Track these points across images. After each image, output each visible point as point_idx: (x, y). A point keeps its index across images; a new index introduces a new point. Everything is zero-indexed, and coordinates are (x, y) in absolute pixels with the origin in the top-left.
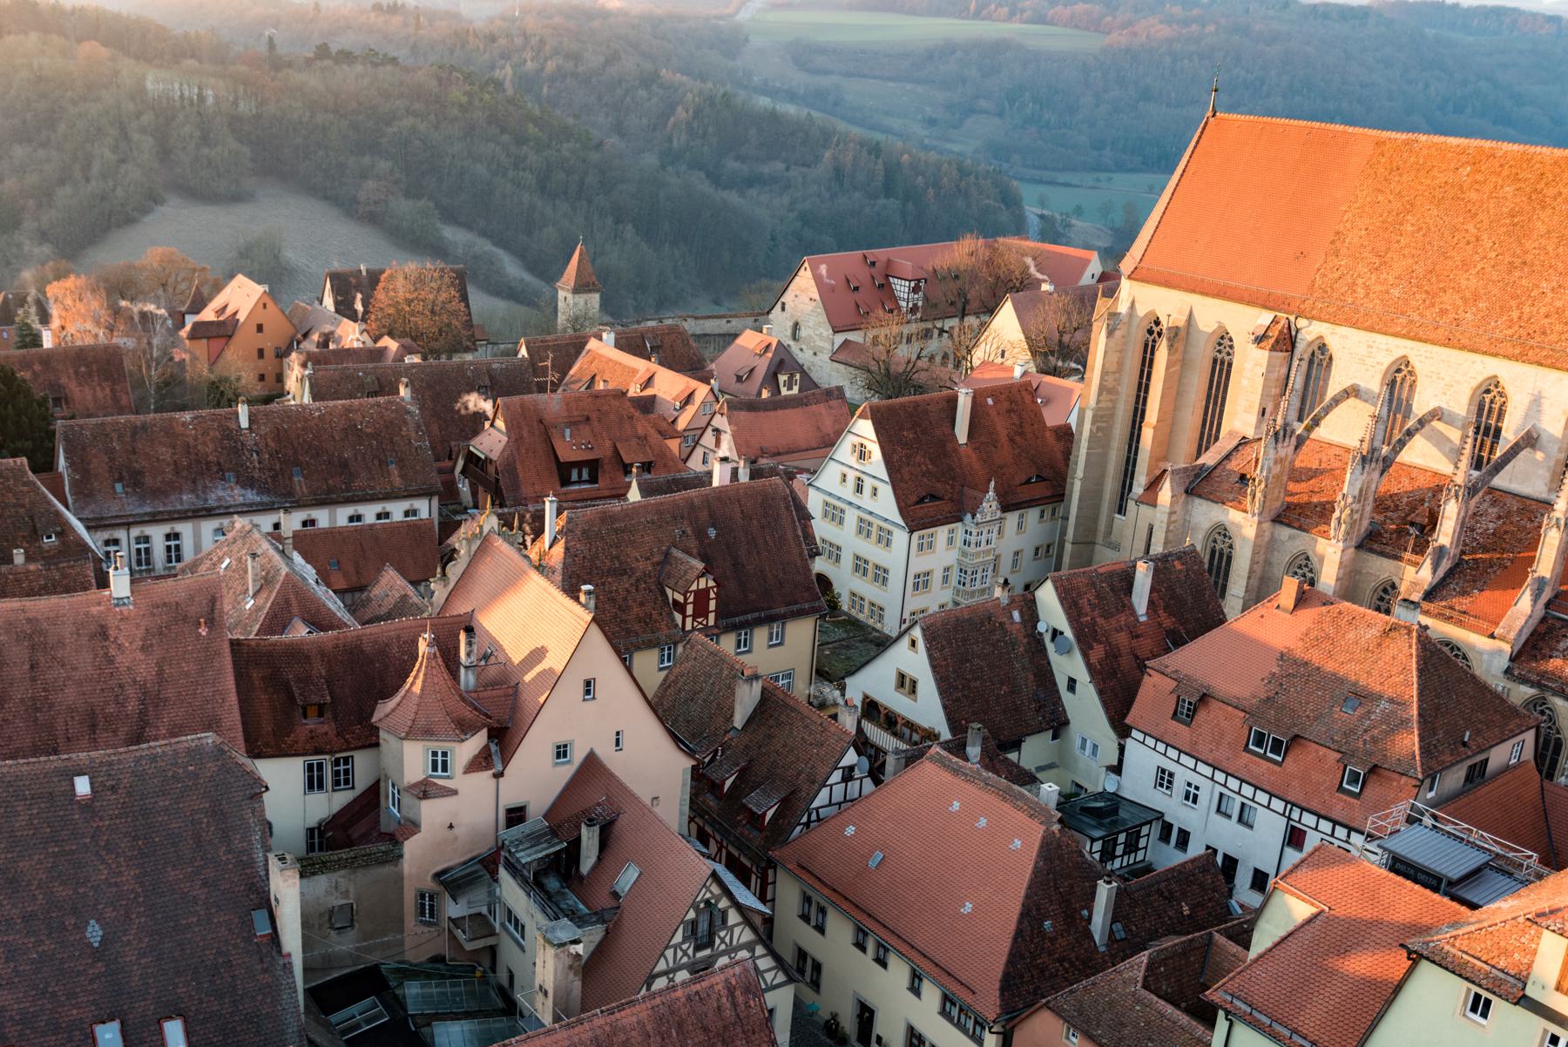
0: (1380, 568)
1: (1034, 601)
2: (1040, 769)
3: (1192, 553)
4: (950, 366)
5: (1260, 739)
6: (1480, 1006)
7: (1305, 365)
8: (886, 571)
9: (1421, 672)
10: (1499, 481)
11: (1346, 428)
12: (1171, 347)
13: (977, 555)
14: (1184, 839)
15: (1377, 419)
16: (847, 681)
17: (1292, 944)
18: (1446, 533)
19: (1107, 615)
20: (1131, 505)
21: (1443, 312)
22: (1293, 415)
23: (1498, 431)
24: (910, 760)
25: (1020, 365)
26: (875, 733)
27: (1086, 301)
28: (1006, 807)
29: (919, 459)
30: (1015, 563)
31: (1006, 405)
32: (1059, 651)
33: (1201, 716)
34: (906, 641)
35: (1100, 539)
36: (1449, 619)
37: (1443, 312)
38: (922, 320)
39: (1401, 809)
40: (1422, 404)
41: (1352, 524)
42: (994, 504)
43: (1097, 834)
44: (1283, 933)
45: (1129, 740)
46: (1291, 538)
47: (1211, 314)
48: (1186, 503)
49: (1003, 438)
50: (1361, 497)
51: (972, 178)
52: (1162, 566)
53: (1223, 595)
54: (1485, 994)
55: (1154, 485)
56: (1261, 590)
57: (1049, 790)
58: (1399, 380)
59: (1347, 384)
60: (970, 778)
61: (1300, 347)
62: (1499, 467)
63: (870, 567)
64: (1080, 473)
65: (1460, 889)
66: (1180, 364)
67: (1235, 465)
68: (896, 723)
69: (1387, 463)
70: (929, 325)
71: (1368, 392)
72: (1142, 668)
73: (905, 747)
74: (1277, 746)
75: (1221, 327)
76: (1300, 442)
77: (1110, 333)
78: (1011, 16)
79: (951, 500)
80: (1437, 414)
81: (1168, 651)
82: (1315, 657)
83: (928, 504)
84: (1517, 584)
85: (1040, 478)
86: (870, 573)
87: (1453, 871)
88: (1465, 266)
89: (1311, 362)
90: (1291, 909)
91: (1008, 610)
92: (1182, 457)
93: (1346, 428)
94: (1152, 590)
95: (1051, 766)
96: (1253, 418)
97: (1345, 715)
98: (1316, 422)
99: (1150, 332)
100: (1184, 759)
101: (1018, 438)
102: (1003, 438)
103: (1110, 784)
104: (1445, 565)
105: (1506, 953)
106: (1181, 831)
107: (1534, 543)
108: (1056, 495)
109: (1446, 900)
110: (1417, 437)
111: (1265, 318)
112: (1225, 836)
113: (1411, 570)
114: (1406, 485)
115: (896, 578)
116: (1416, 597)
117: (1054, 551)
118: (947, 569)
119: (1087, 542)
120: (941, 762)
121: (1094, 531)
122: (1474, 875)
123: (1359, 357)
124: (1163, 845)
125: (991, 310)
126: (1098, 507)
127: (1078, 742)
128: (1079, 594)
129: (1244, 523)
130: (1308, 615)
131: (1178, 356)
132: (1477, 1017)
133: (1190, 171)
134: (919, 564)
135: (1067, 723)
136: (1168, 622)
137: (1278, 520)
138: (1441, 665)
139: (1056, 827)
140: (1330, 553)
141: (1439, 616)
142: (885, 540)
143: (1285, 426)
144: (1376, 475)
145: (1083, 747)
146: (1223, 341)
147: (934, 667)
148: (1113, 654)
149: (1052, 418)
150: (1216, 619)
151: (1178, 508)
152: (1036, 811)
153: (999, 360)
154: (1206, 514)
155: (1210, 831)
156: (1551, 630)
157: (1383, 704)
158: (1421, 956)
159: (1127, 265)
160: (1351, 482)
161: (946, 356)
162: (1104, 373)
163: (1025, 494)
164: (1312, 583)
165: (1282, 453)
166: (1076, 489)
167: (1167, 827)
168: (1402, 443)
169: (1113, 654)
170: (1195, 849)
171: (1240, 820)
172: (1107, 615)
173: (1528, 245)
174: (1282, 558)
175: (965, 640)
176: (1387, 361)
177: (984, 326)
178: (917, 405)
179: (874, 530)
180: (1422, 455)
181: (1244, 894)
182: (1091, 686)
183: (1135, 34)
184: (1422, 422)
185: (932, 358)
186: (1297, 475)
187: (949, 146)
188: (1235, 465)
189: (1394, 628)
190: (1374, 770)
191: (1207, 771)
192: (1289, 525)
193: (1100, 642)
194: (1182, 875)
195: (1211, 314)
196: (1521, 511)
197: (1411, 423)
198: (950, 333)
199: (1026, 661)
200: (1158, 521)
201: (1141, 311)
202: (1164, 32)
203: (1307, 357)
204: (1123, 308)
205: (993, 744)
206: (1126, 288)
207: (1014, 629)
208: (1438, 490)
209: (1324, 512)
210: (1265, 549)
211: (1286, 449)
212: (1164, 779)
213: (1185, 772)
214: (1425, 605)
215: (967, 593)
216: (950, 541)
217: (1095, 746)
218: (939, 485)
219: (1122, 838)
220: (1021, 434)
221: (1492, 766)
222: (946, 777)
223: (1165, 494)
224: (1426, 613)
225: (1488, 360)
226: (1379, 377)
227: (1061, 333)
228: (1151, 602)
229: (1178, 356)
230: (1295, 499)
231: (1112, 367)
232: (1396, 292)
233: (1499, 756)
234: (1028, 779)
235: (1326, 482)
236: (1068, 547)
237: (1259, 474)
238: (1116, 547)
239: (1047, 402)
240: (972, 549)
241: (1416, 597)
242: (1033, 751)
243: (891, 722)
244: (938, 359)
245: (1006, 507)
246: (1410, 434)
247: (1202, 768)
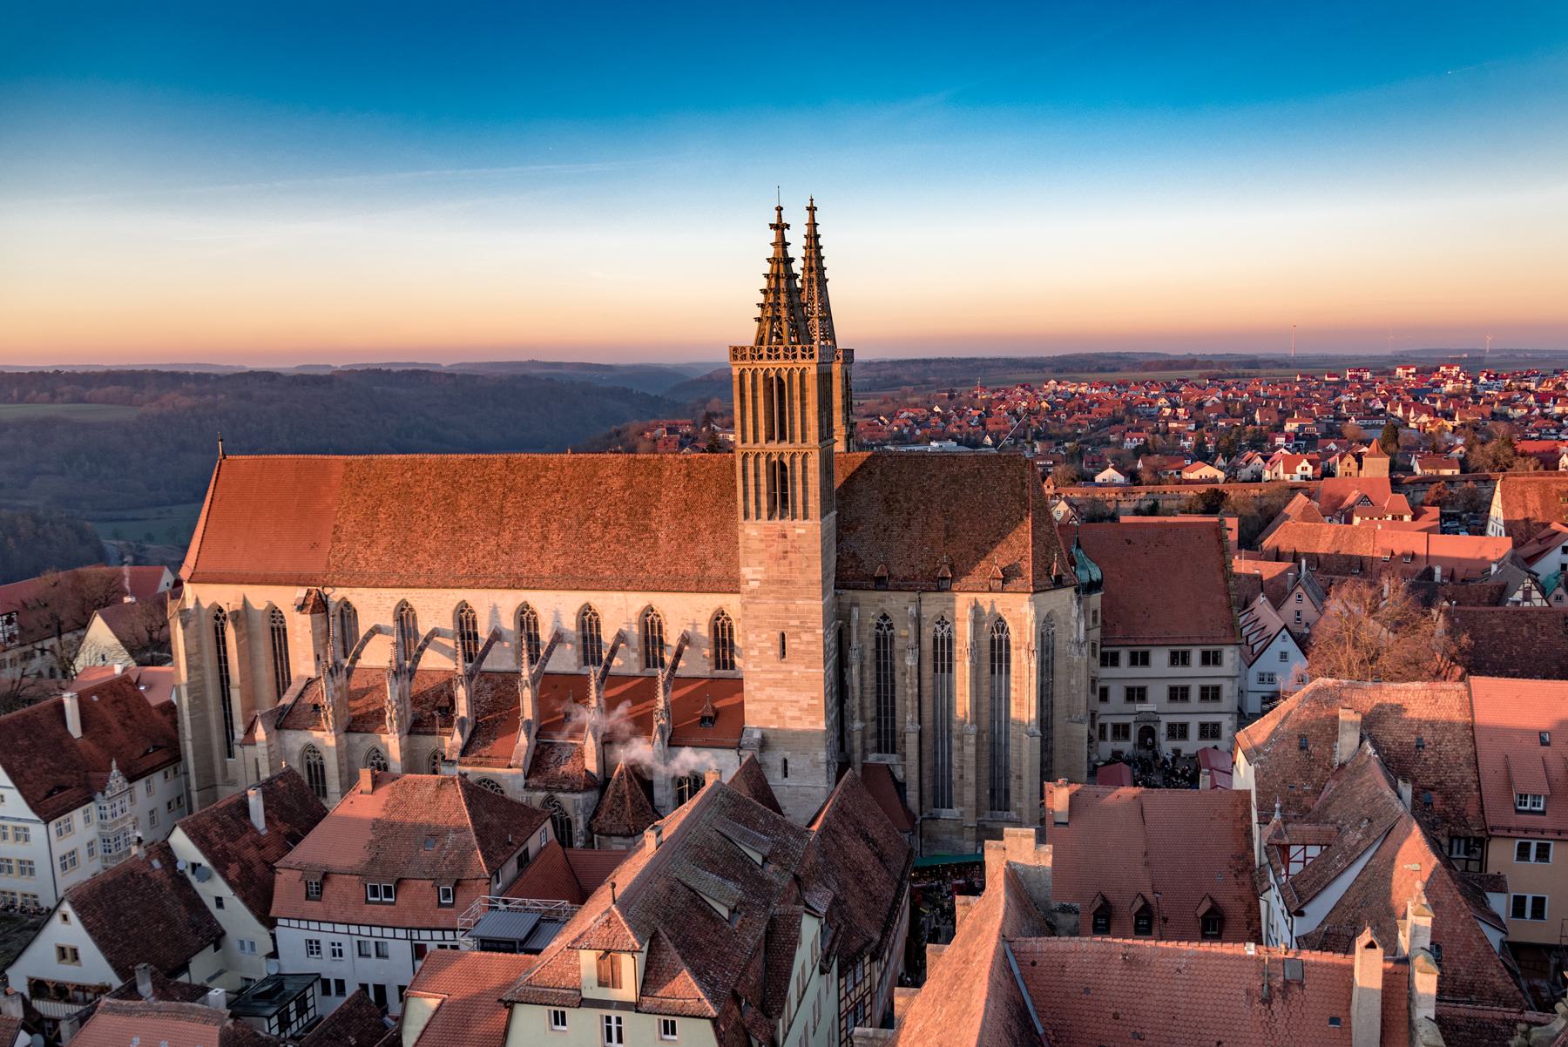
0: (427, 743)
1: (169, 847)
2: (210, 979)
3: (289, 774)
4: (59, 677)
5: (375, 893)
6: (559, 1019)
7: (338, 619)
8: (30, 863)
9: (469, 806)
10: (486, 666)
11: (378, 655)
12: (235, 626)
13: (116, 823)
14: (341, 985)
15: (396, 644)
16: (8, 972)
17: (431, 1033)
18: (462, 709)
19: (234, 839)
20: (237, 749)
21: (420, 566)
22: (340, 655)
23: (476, 635)
24: (83, 1019)
25: (120, 664)
26: (44, 1007)
27: (162, 606)
28: (182, 1024)
29: (38, 760)
30: (152, 820)
31: (111, 698)
32: (202, 879)
33: (328, 889)
34: (57, 918)
35: (219, 781)
36: (480, 764)
37: (420, 566)
38: (22, 645)
39: (478, 904)
40: (424, 628)
41: (400, 719)
42: (121, 779)
43: (270, 1011)
44: (421, 1028)
45: (278, 929)
46: (362, 740)
47: (259, 597)
48: (278, 737)
49: (115, 724)
50: (401, 700)
51: (48, 525)
52: (268, 789)
53: (325, 795)
54: (560, 1009)
55: (250, 729)
56: (350, 781)
57: (217, 994)
58: (404, 616)
59: (371, 626)
60: (143, 1014)
61: (332, 607)
62: (482, 658)
63: (14, 864)
64: (188, 735)
65: (527, 945)
66: (246, 638)
67: (308, 699)
68: (67, 991)
69: (412, 672)
70: (28, 648)
71: (387, 628)
72: (272, 869)
73: (77, 1008)
74: (388, 893)
75: (271, 604)
76: (349, 672)
77: (184, 626)
78: (53, 398)
79: (79, 786)
80: (435, 633)
81: (290, 849)
82: (396, 817)
83: (57, 795)
84: (515, 729)
85: (156, 748)
86: (15, 870)
87: (521, 934)
88: (425, 534)
89: (342, 616)
90: (423, 1007)
91: (148, 861)
92: (267, 703)
93: (378, 655)
94: (266, 808)
95: (220, 973)
96: (312, 664)
97: (428, 853)
98: (357, 656)
99: (217, 618)
100: (324, 926)
101: (128, 722)
102: (115, 724)
103: (271, 968)
104: (468, 729)
105: (563, 975)
106: (337, 981)
107: (517, 701)
108: (176, 757)
109: (521, 955)
110: (427, 650)
111: (301, 592)
112: (371, 971)
113: (447, 739)
114: (428, 684)
115: (42, 867)
116: (455, 756)
117: (184, 800)
118: (90, 844)
119: (209, 786)
120: (113, 1010)
121: (213, 776)
122: (535, 930)
123: (374, 607)
124: (326, 998)
125: (84, 625)
126: (211, 758)
127: (237, 945)
128: (207, 830)
129: (326, 738)
130: (384, 792)
131: (244, 631)
132: (560, 1027)
133: (218, 495)
134: (61, 847)
135: (223, 933)
136: (285, 828)
137: (349, 730)
138: (481, 795)
139: (229, 1023)
140: (392, 742)
141: (474, 764)
142: (22, 835)
143: (335, 663)
144: (407, 682)
145: (242, 948)
146: (274, 613)
147: (90, 931)
148: (247, 867)
149: (155, 699)
150: (322, 813)
151: (273, 741)
152: (207, 1018)
153: (101, 663)
154: (296, 740)
155: (357, 972)
156: (543, 752)
157: (452, 836)
158: (513, 1002)
159: (185, 573)
160: (391, 692)
161: (52, 670)
162: (188, 656)
163: (146, 764)
164: (386, 768)
165: (339, 683)
166: (189, 748)
167: (326, 983)
168: (418, 657)
169: (247, 867)
170: (351, 989)
171: (378, 955)
172: (234, 839)
173: (460, 515)
174: (360, 756)
175: (113, 899)
176: (393, 605)
177: (81, 639)
178: (25, 716)
179: (10, 831)
180: (434, 661)
181: (394, 1007)
182: (236, 899)
183: (162, 405)
184: (427, 640)
185: (40, 674)
186: (355, 695)
187: (20, 503)
188: (308, 699)
189: (444, 782)
190: (458, 883)
191: (343, 928)
192: (358, 732)
193: (233, 861)
194: (343, 1016)
195: (259, 597)
196: (505, 681)
197: (420, 642)
198: (52, 650)
199: (175, 898)
200: (260, 753)
201: (205, 604)
202: (187, 402)
203: (338, 613)
204: (190, 605)
205: (161, 975)
206: (189, 590)
207: (157, 875)
208: (449, 682)
209: (380, 715)
210: (345, 753)
211: (341, 679)
212: (313, 947)
213: (326, 935)
214: (463, 760)
215: (113, 857)
216: (87, 820)
217: (252, 944)
218: (63, 777)
219: (292, 1006)
220: (131, 718)
221: (531, 852)
222: (121, 1020)
223: (260, 733)
224: (466, 764)
225: (456, 591)
226: (391, 617)
227: (150, 632)
228: (267, 818)
229: (244, 631)
230: (357, 713)
231: (194, 650)
232: (386, 559)
233: (534, 844)
234: (200, 992)
235: (376, 695)
236: (195, 795)
237: (324, 701)
238: (233, 783)
239: (150, 687)
240: (110, 820)
241: (455, 756)
242: (200, 967)
243: (61, 992)
244: (46, 673)
245: (132, 779)
246: (421, 649)
247: (339, 928)
